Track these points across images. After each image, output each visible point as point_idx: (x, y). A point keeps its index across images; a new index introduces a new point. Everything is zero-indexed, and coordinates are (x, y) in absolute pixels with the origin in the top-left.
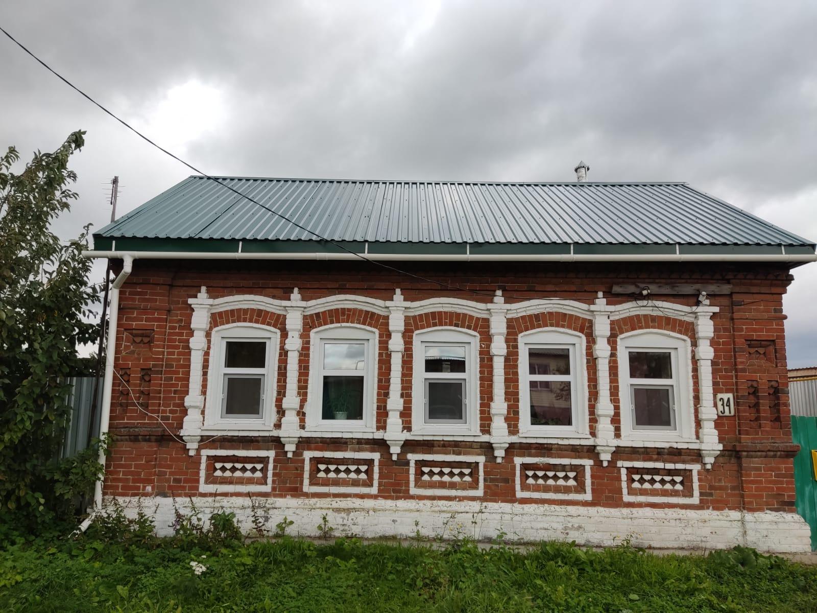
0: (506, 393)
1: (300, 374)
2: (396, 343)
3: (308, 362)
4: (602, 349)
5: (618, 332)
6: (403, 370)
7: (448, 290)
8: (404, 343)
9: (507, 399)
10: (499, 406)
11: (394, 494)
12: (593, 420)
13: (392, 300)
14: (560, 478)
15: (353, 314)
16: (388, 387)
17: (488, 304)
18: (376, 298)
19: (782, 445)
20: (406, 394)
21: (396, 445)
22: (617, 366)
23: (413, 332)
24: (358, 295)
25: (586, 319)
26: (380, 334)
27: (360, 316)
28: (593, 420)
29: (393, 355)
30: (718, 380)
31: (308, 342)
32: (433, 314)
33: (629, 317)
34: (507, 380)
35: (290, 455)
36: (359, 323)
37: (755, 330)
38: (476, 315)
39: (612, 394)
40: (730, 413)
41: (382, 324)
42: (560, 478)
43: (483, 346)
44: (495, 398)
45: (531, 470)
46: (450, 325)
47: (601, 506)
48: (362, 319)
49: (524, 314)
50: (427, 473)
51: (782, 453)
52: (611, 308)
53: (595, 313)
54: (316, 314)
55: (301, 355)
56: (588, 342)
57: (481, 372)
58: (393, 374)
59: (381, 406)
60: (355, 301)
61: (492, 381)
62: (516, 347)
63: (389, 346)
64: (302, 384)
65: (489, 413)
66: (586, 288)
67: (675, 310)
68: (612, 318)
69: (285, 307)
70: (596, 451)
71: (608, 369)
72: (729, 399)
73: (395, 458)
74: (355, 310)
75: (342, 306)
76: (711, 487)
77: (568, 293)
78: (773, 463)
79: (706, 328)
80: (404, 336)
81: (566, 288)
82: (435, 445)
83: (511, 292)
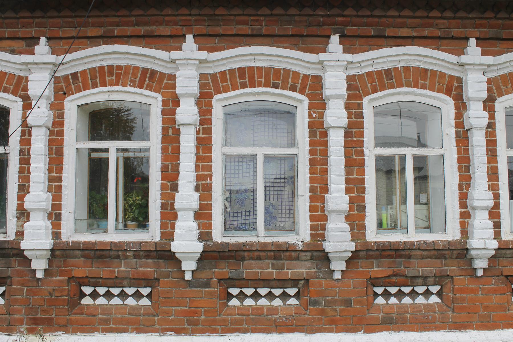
0: (347, 181)
1: (51, 161)
2: (187, 112)
3: (61, 142)
4: (476, 116)
5: (496, 95)
6: (198, 151)
7: (261, 36)
8: (200, 112)
9: (348, 191)
10: (337, 198)
11: (188, 327)
12: (466, 215)
14: (419, 294)
15: (125, 73)
16: (176, 177)
17: (321, 54)
18: (157, 49)
20: (203, 186)
21: (190, 259)
22: (496, 141)
23: (211, 97)
24: (131, 45)
25: (454, 77)
26: (163, 101)
27: (134, 75)
28: (466, 215)
29: (183, 130)
31: (62, 115)
32: (241, 70)
34: (348, 163)
35: (40, 275)
36: (134, 86)
38: (303, 71)
39: (490, 179)
41: (167, 87)
42: (419, 294)
43: (314, 115)
44: (332, 187)
45: (381, 286)
46: (266, 86)
47: (474, 329)
48: (137, 80)
49: (370, 69)
50: (236, 297)
52: (489, 60)
53: (467, 67)
54: (72, 74)
55: (51, 133)
56: (457, 108)
57: (311, 152)
58: (182, 157)
59: (166, 204)
60: (127, 53)
61: (327, 164)
62: (360, 115)
63: (177, 117)
64: (54, 174)
65: (323, 211)
66: (454, 33)
69: (26, 64)
70: (468, 256)
71: (485, 144)
73: (188, 276)
74: (128, 67)
75: (110, 63)
77: (430, 41)
80: (199, 103)
81: (426, 32)
82: (247, 257)
83: (352, 39)
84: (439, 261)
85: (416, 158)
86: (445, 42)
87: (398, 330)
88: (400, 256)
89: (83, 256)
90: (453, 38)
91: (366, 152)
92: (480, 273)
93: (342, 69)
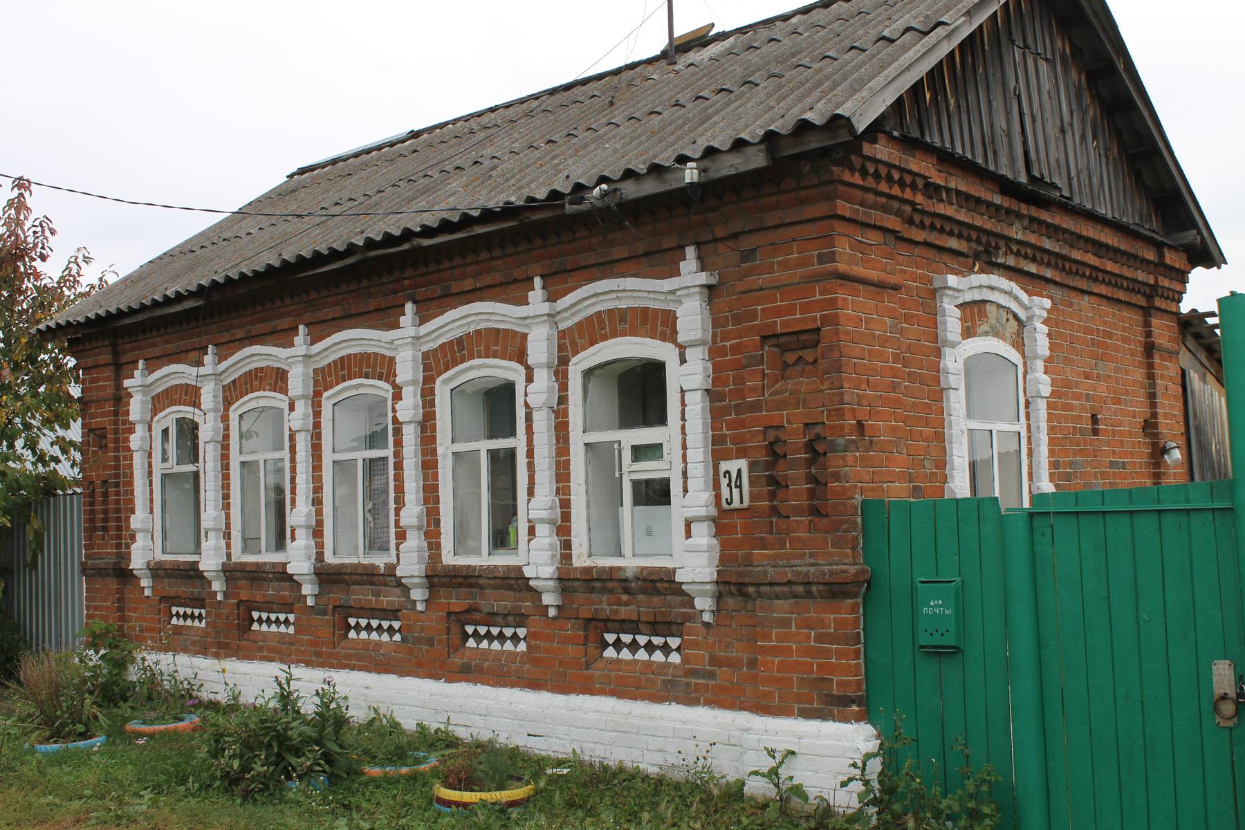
13: (292, 345)
19: (812, 569)
22: (567, 423)
30: (725, 431)
33: (587, 319)
35: (220, 597)
37: (779, 312)
40: (742, 502)
51: (821, 587)
66: (517, 274)
67: (649, 292)
68: (562, 326)
72: (739, 471)
76: (714, 661)
78: (813, 610)
79: (692, 318)
81: (488, 280)
84: (511, 593)
85: (493, 455)
86: (513, 286)
87: (475, 682)
88: (471, 586)
89: (245, 578)
90: (516, 281)
91: (440, 450)
92: (552, 612)
93: (410, 347)
